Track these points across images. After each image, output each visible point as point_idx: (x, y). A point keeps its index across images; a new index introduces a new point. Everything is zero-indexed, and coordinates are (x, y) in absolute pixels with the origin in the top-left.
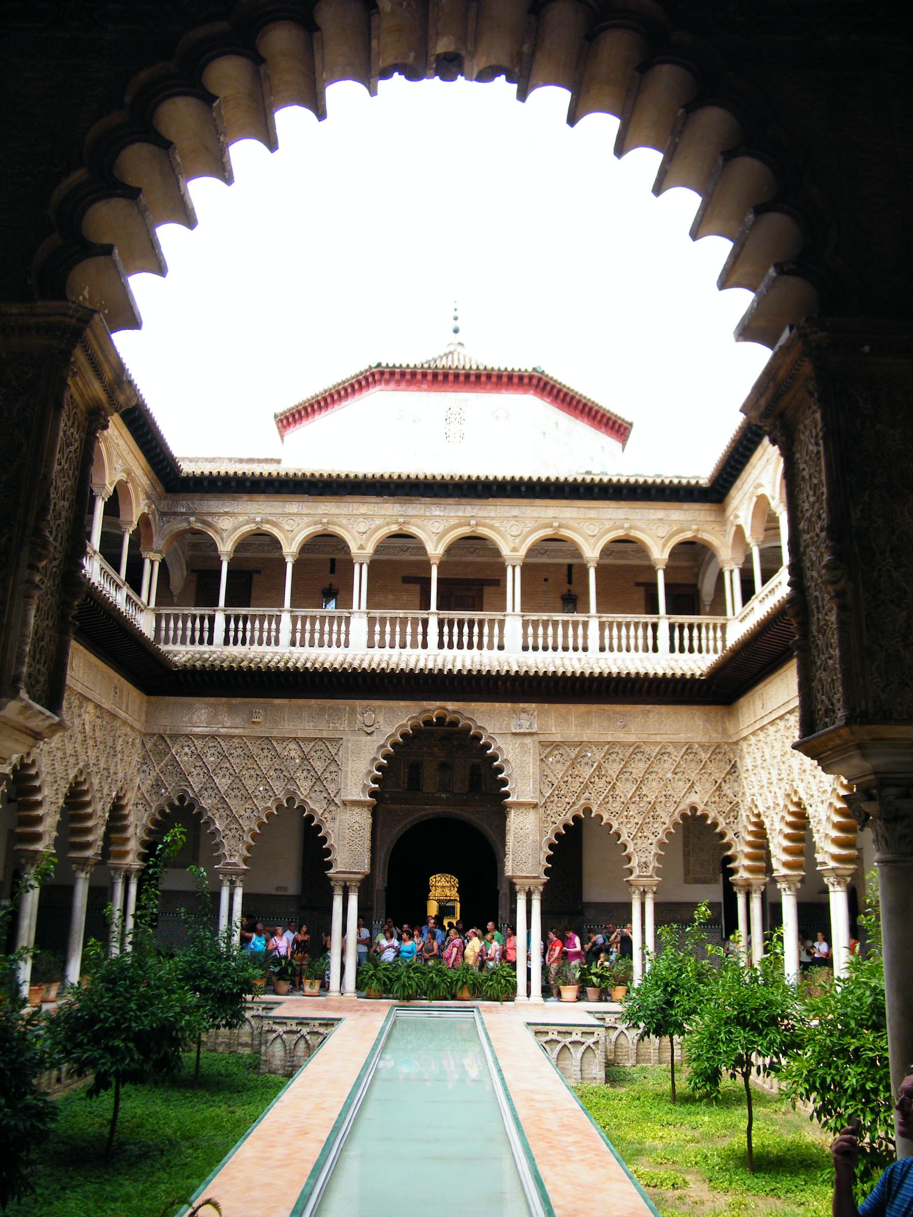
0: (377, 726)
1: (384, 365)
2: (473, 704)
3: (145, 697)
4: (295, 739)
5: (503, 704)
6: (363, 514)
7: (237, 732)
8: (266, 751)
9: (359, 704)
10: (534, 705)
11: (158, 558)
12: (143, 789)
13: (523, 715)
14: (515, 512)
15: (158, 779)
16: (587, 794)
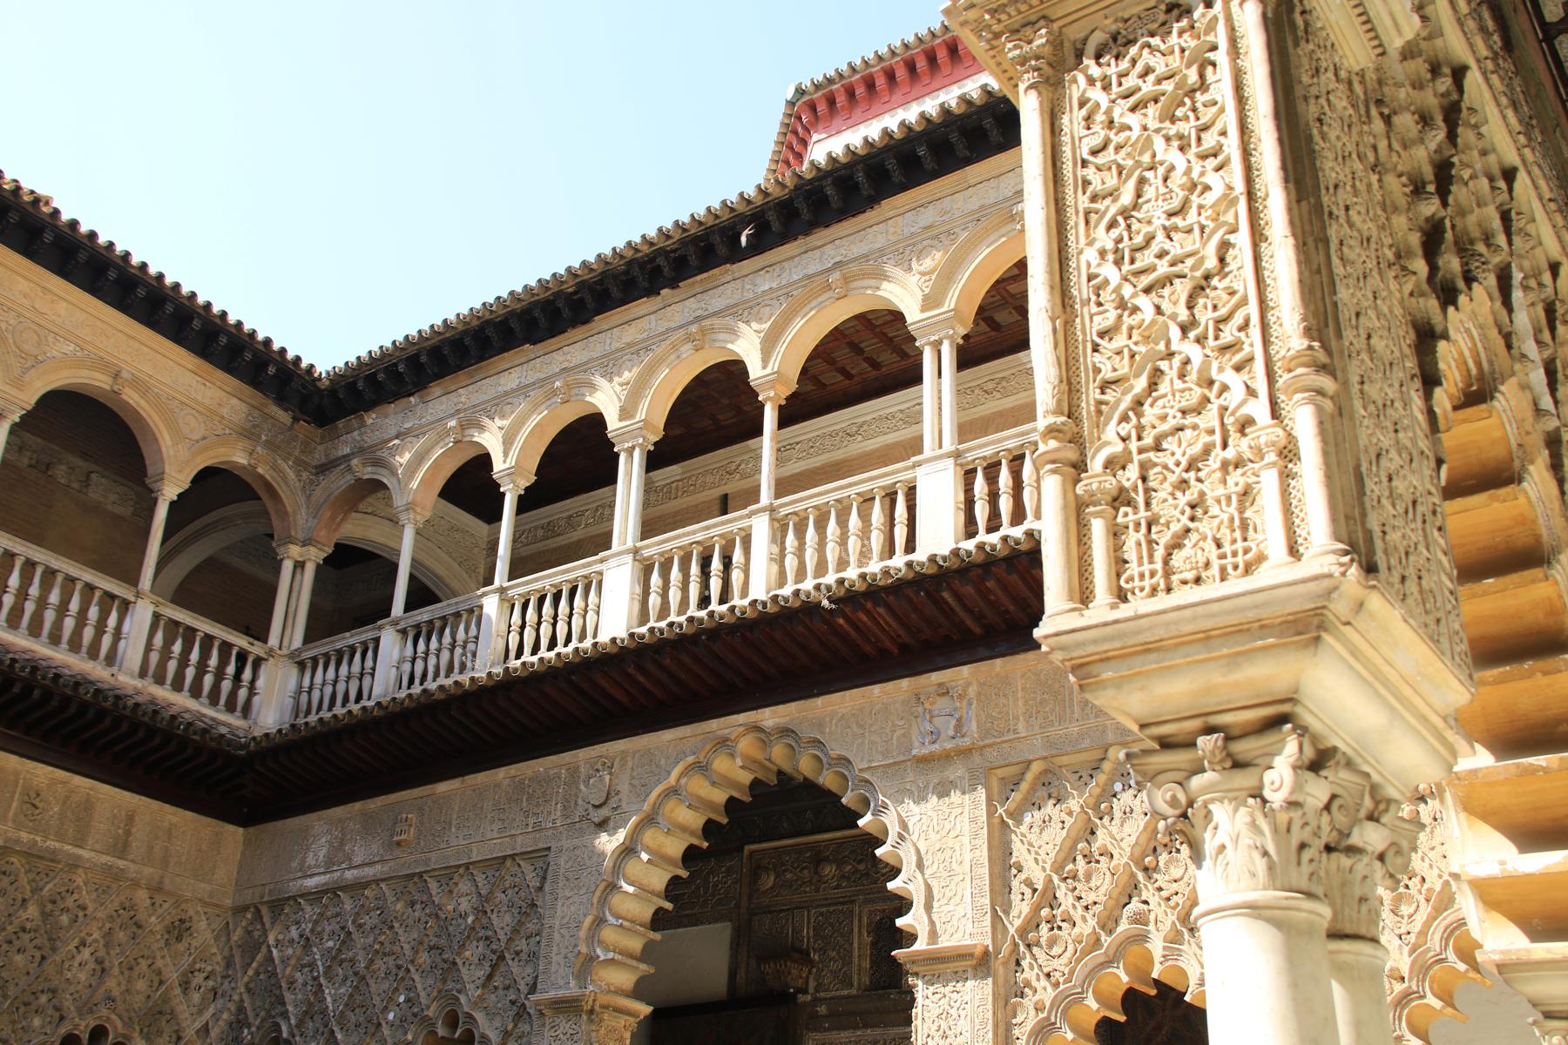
0: (613, 803)
1: (811, 88)
2: (819, 701)
3: (234, 834)
4: (467, 866)
5: (890, 685)
6: (630, 345)
7: (369, 872)
8: (418, 906)
9: (583, 756)
10: (965, 670)
11: (315, 556)
12: (215, 1032)
13: (942, 704)
14: (928, 216)
15: (241, 1009)
16: (1135, 905)
